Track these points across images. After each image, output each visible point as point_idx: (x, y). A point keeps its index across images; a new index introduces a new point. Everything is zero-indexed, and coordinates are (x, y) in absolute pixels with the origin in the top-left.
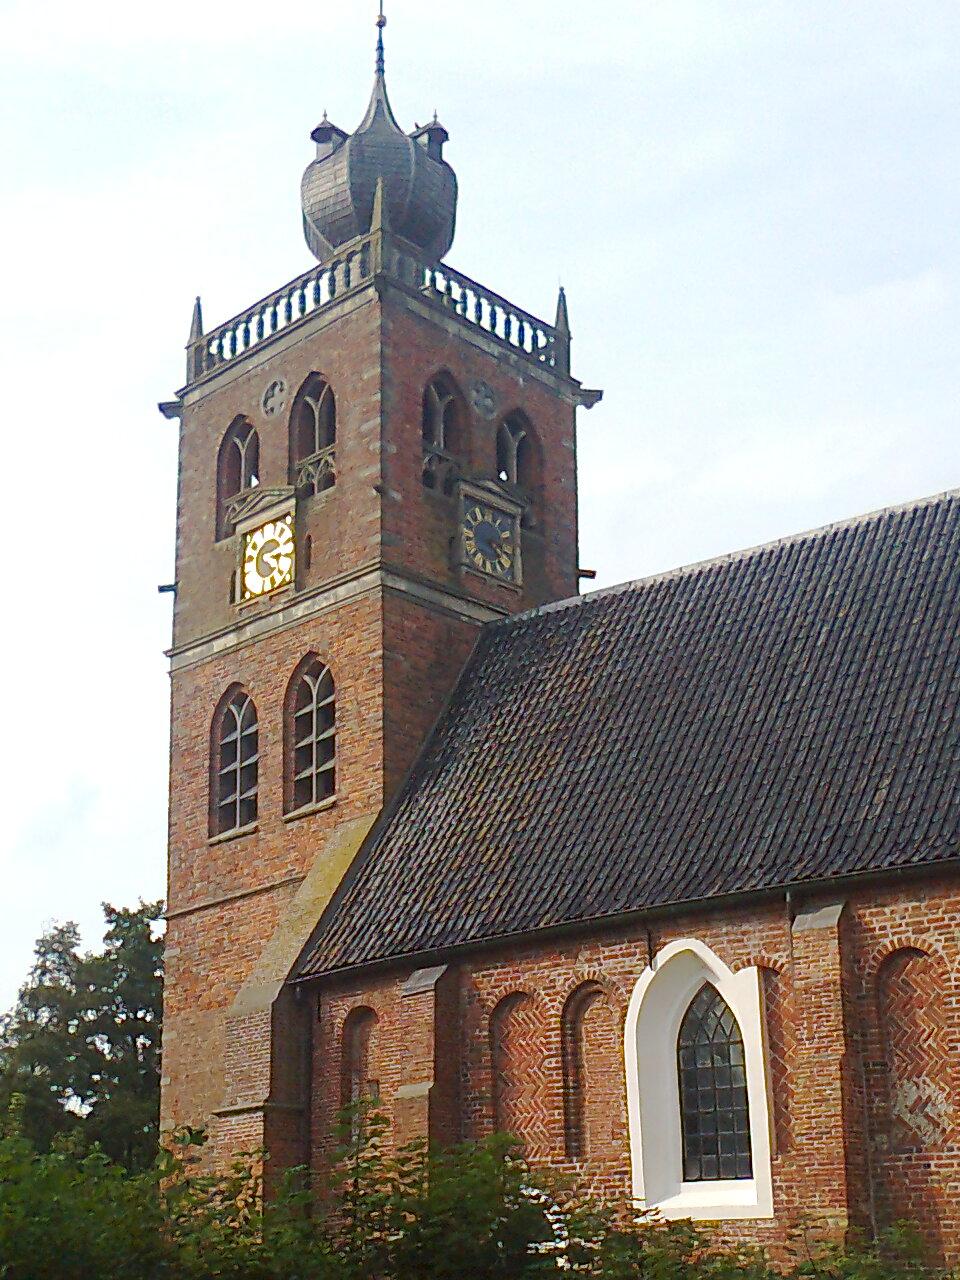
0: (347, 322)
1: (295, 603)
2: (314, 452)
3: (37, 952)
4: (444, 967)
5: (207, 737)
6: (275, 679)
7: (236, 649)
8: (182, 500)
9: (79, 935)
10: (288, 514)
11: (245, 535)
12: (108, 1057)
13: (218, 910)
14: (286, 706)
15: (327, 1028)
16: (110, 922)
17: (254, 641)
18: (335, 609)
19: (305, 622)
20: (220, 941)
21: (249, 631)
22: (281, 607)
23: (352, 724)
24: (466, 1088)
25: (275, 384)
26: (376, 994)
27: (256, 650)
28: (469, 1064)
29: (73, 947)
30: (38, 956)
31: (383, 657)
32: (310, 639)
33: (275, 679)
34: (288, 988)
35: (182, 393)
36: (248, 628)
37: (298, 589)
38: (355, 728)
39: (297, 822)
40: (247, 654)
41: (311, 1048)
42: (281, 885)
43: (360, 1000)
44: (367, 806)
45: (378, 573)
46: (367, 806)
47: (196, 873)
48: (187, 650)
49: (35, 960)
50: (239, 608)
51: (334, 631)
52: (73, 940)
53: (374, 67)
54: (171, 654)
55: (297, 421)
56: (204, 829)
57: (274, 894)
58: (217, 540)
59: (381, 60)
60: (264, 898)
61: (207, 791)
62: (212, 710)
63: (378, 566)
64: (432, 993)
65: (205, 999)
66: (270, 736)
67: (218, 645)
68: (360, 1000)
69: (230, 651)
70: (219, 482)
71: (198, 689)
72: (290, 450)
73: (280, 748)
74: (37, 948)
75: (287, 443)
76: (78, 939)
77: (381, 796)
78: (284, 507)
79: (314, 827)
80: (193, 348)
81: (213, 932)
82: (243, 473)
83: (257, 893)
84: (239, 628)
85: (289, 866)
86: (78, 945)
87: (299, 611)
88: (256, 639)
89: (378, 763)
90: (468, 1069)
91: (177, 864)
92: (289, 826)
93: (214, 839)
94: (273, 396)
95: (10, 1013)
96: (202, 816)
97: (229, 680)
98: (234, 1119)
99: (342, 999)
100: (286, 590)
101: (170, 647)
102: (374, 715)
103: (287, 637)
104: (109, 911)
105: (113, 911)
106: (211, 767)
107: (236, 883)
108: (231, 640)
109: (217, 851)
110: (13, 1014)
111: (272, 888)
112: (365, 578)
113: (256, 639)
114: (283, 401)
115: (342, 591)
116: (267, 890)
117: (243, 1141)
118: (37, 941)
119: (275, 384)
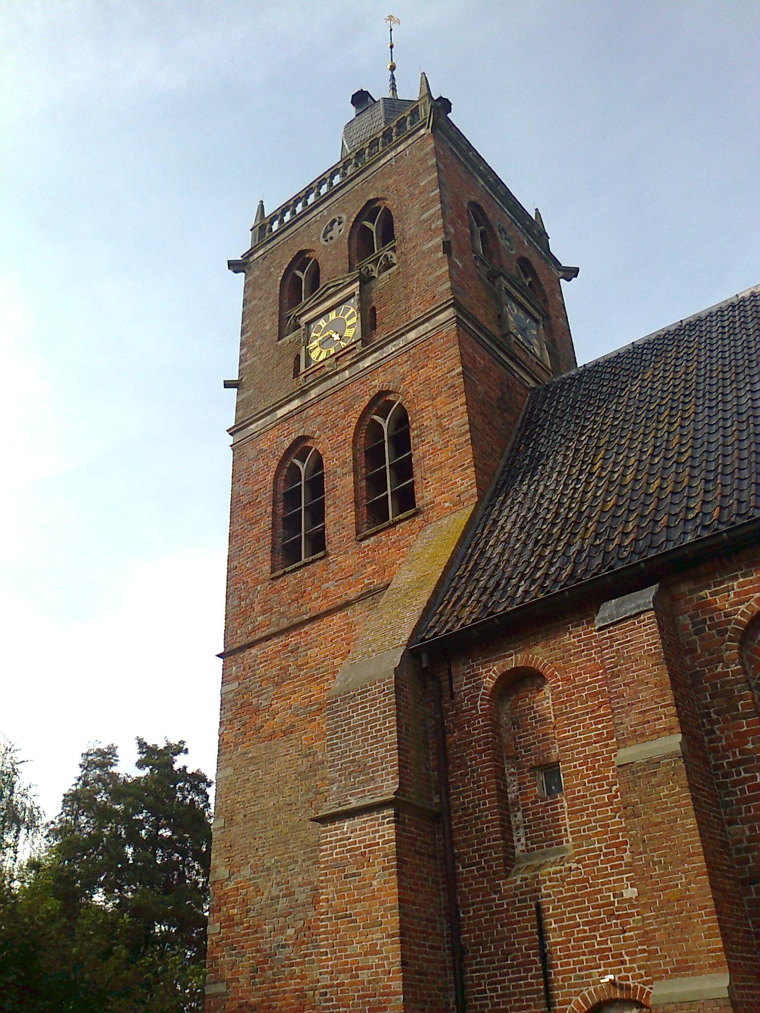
0: (402, 157)
1: (362, 357)
2: (374, 252)
3: (81, 766)
4: (657, 585)
5: (270, 487)
6: (342, 423)
7: (301, 410)
8: (244, 324)
9: (117, 757)
10: (353, 295)
11: (308, 324)
12: (131, 862)
13: (282, 638)
14: (355, 443)
15: (466, 705)
16: (140, 753)
17: (320, 398)
18: (405, 351)
19: (372, 370)
20: (285, 669)
21: (313, 394)
22: (348, 363)
23: (434, 437)
24: (715, 750)
25: (334, 221)
26: (538, 649)
27: (320, 407)
28: (714, 716)
29: (111, 766)
30: (82, 769)
31: (463, 373)
32: (378, 383)
33: (342, 423)
34: (412, 653)
35: (250, 254)
36: (312, 392)
37: (365, 343)
38: (436, 439)
39: (372, 539)
40: (312, 412)
41: (442, 733)
42: (359, 599)
43: (514, 660)
44: (458, 504)
45: (451, 309)
46: (458, 504)
47: (258, 608)
48: (251, 424)
49: (79, 772)
50: (304, 375)
51: (406, 368)
52: (112, 761)
53: (389, 83)
54: (232, 432)
55: (355, 240)
56: (267, 568)
57: (349, 611)
58: (279, 339)
59: (393, 84)
60: (337, 618)
61: (269, 533)
62: (275, 464)
63: (452, 301)
64: (651, 614)
65: (267, 730)
66: (338, 470)
67: (280, 413)
68: (514, 660)
69: (294, 413)
70: (281, 301)
71: (261, 451)
72: (349, 257)
73: (350, 478)
74: (81, 762)
75: (347, 253)
76: (117, 760)
77: (475, 490)
78: (348, 290)
79: (393, 538)
80: (257, 228)
81: (277, 661)
82: (303, 289)
83: (329, 613)
84: (304, 392)
85: (368, 578)
86: (116, 765)
87: (367, 362)
88: (321, 397)
89: (469, 459)
90: (713, 723)
91: (236, 603)
92: (366, 542)
93: (274, 575)
94: (331, 230)
95: (54, 820)
96: (264, 556)
97: (294, 436)
98: (346, 825)
99: (483, 664)
100: (355, 348)
101: (233, 424)
102: (459, 421)
103: (354, 387)
104: (142, 744)
105: (145, 743)
106: (274, 513)
107: (303, 609)
108: (296, 403)
109: (279, 583)
110: (57, 821)
111: (348, 604)
112: (437, 318)
113: (321, 397)
114: (340, 232)
115: (412, 335)
116: (340, 608)
117: (362, 854)
118: (82, 754)
119: (334, 221)
